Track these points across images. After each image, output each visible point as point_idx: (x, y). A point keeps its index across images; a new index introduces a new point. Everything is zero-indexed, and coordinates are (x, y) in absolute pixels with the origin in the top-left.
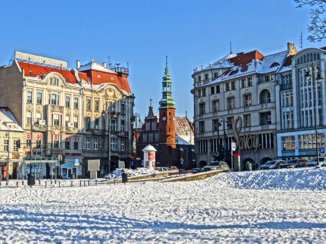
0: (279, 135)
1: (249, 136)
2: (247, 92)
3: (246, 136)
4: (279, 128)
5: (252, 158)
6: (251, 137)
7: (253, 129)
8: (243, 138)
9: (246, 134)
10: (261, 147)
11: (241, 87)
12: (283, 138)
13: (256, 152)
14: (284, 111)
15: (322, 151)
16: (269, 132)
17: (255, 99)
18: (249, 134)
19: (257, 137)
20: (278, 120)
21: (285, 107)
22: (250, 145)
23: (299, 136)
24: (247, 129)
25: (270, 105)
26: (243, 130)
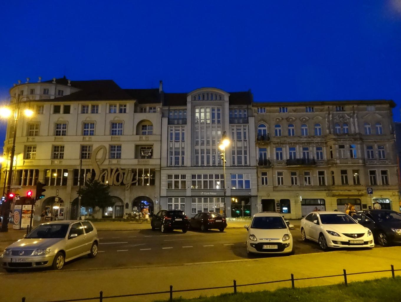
0: (164, 174)
1: (117, 170)
2: (116, 119)
3: (112, 170)
4: (164, 164)
5: (121, 198)
6: (121, 172)
7: (122, 162)
8: (108, 172)
9: (113, 167)
10: (135, 184)
11: (108, 112)
12: (170, 176)
13: (127, 190)
14: (171, 146)
15: (369, 192)
16: (149, 168)
17: (129, 128)
18: (119, 167)
19: (130, 172)
20: (164, 154)
21: (173, 142)
22: (118, 180)
23: (194, 176)
24: (114, 161)
25: (151, 138)
26: (107, 162)
